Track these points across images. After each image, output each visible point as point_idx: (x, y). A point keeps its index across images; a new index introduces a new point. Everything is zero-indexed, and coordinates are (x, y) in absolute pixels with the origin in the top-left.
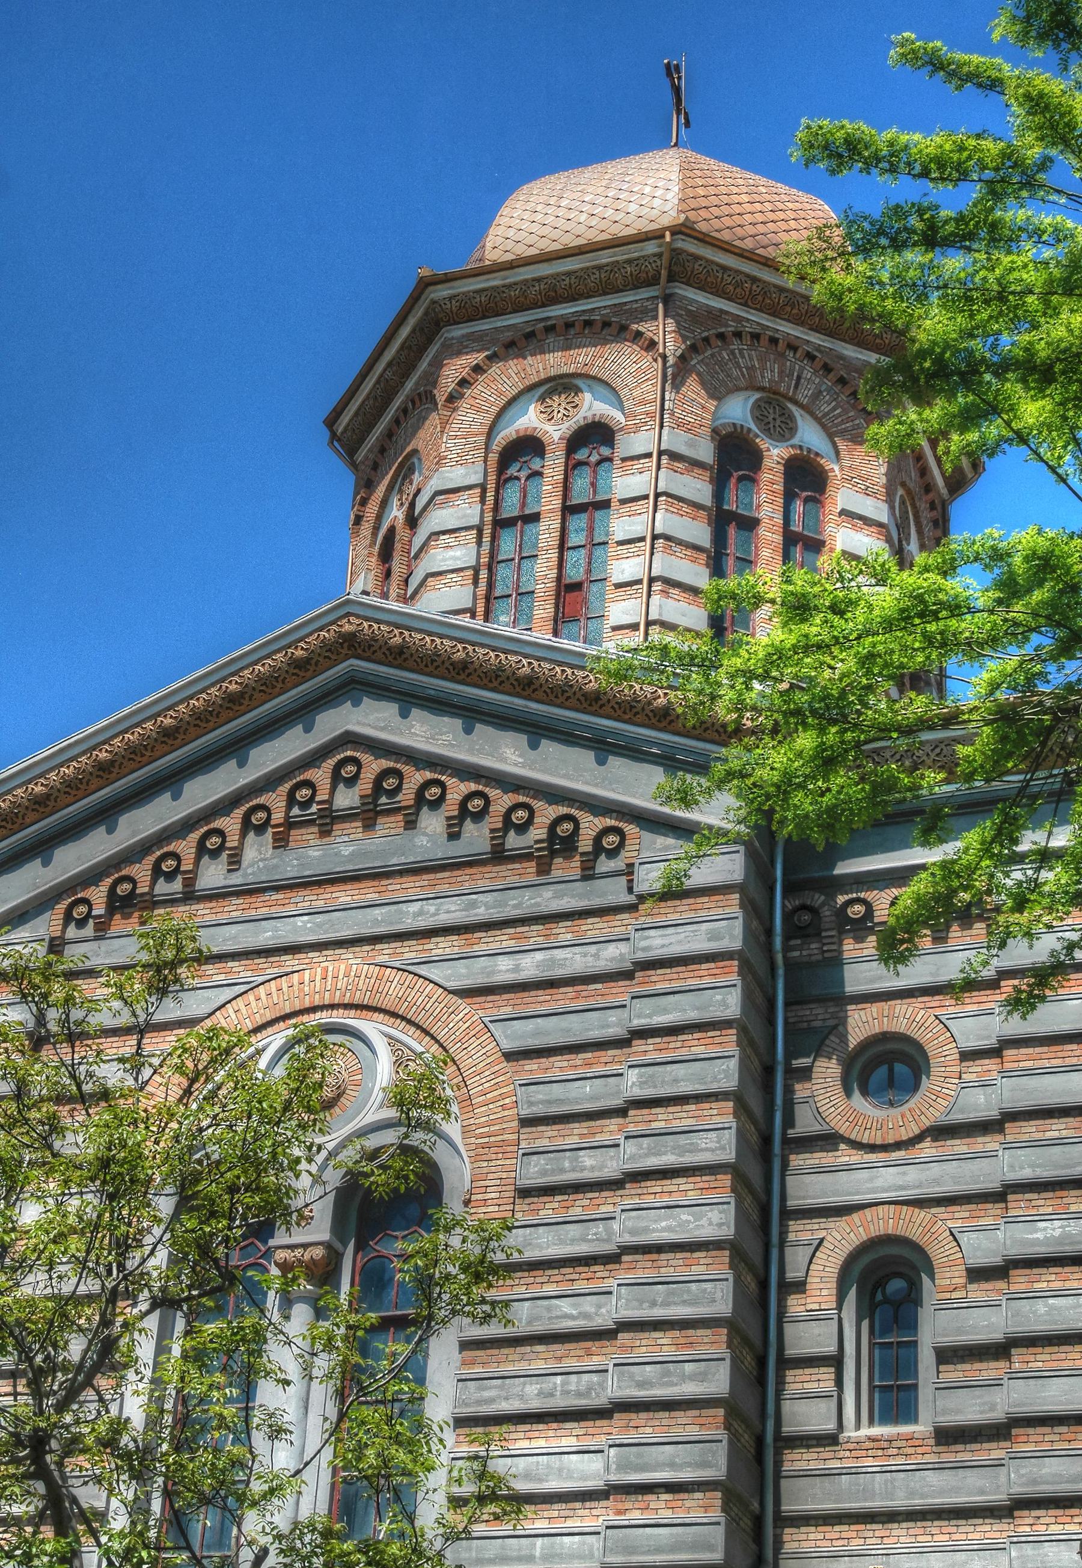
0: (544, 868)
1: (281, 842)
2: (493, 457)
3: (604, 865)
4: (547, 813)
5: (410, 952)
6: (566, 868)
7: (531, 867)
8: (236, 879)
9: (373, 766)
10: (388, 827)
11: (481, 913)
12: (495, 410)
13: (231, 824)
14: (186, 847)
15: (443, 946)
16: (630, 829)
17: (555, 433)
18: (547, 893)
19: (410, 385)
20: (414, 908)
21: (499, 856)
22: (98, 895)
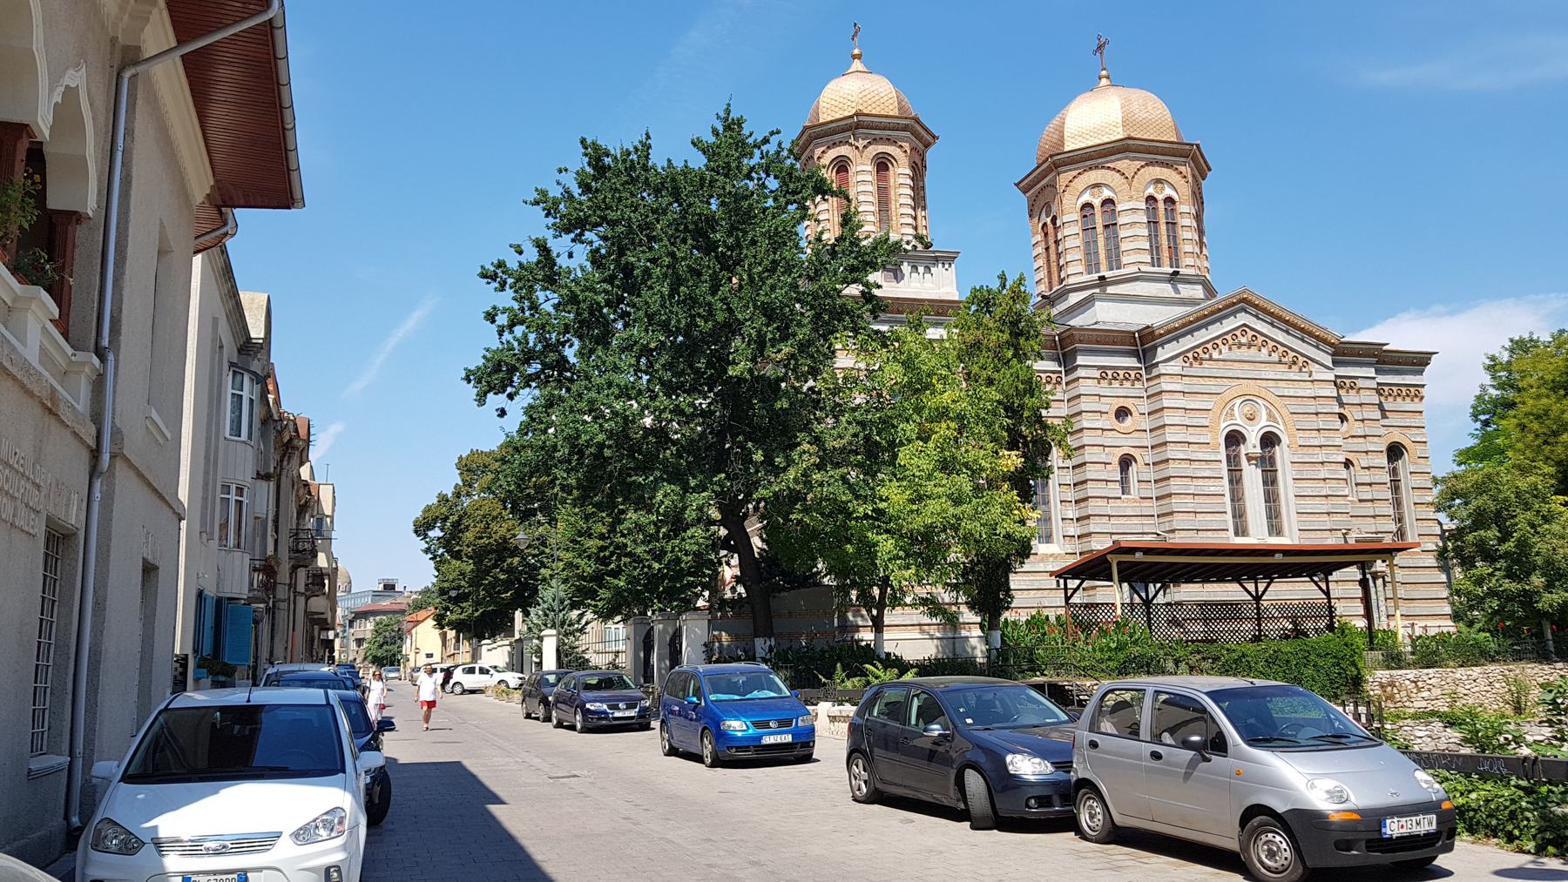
0: (1290, 367)
1: (1230, 349)
3: (1304, 370)
4: (1292, 354)
5: (1264, 383)
6: (1295, 368)
8: (1221, 357)
9: (1251, 333)
13: (1219, 342)
15: (1271, 384)
21: (1280, 362)
22: (1190, 355)
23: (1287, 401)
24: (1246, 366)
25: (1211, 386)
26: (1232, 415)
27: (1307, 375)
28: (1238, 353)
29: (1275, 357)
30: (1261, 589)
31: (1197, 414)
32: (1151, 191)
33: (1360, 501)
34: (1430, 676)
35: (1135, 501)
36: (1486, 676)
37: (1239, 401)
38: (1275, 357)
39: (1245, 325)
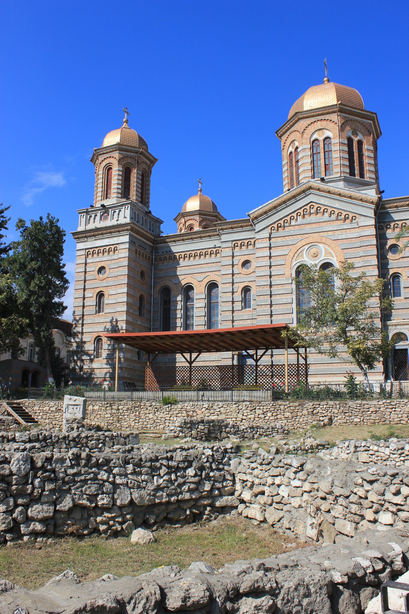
2: (311, 143)
6: (348, 221)
7: (342, 221)
8: (297, 223)
10: (319, 215)
11: (335, 229)
12: (310, 135)
13: (295, 215)
14: (288, 218)
16: (357, 216)
17: (321, 138)
18: (345, 225)
19: (293, 128)
20: (325, 228)
21: (337, 220)
23: (340, 242)
24: (314, 226)
25: (289, 240)
26: (302, 256)
27: (356, 224)
28: (308, 219)
29: (334, 217)
30: (258, 357)
31: (279, 258)
32: (315, 136)
33: (405, 298)
34: (219, 407)
35: (250, 311)
36: (261, 408)
37: (307, 247)
38: (334, 217)
39: (311, 202)
